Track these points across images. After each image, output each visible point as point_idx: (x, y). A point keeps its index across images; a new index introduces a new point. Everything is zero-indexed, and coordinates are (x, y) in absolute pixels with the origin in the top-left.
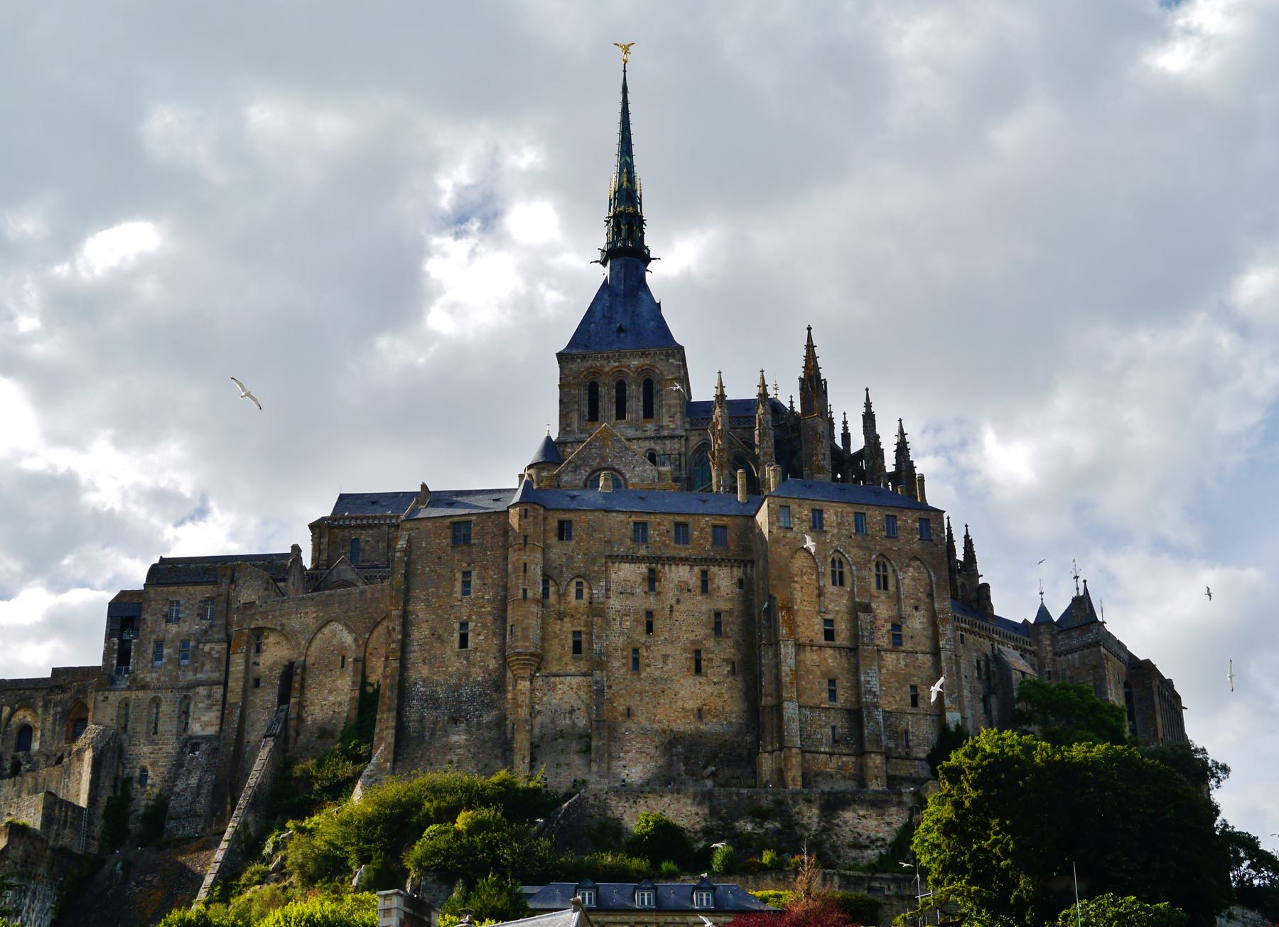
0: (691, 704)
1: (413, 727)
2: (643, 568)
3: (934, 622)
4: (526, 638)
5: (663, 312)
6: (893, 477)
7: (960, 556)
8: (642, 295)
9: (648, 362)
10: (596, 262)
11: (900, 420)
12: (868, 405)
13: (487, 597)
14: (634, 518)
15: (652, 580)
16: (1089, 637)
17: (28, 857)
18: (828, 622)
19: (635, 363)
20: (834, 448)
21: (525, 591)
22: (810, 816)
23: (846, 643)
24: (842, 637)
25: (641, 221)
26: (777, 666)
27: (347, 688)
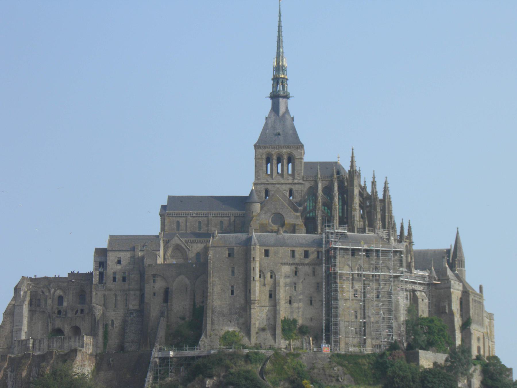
2: (293, 267)
4: (255, 295)
5: (295, 123)
7: (406, 233)
8: (287, 116)
9: (290, 150)
10: (268, 97)
11: (386, 178)
12: (374, 178)
13: (240, 277)
14: (290, 249)
17: (82, 359)
19: (284, 150)
20: (360, 186)
21: (254, 277)
25: (287, 79)
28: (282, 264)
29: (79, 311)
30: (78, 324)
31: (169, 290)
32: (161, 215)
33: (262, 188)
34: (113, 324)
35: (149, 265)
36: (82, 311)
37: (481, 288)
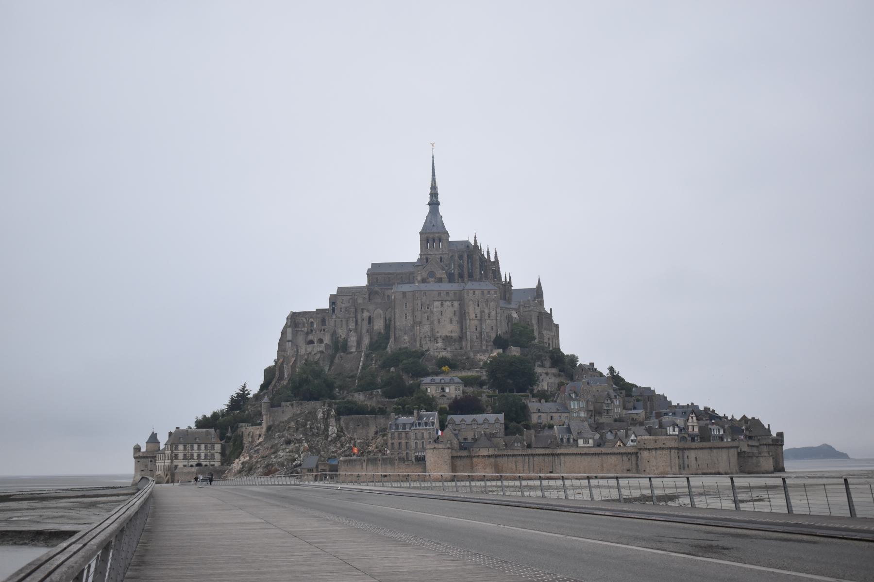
0: (450, 330)
1: (397, 335)
2: (440, 302)
3: (497, 314)
5: (443, 219)
6: (493, 263)
7: (508, 280)
8: (438, 215)
12: (488, 249)
13: (410, 309)
15: (442, 305)
16: (530, 309)
18: (476, 314)
19: (437, 235)
22: (472, 354)
23: (480, 319)
24: (479, 318)
25: (438, 194)
26: (466, 324)
27: (382, 322)
28: (434, 301)
29: (322, 331)
30: (322, 338)
31: (372, 317)
32: (367, 274)
33: (425, 257)
34: (341, 337)
35: (360, 303)
36: (324, 330)
37: (551, 310)
